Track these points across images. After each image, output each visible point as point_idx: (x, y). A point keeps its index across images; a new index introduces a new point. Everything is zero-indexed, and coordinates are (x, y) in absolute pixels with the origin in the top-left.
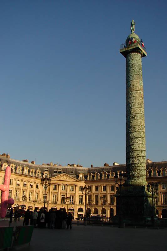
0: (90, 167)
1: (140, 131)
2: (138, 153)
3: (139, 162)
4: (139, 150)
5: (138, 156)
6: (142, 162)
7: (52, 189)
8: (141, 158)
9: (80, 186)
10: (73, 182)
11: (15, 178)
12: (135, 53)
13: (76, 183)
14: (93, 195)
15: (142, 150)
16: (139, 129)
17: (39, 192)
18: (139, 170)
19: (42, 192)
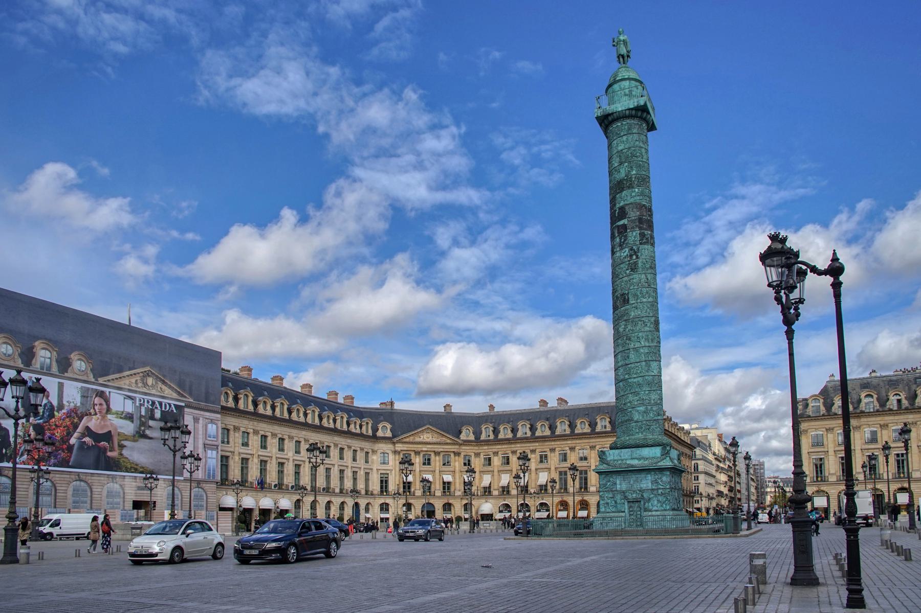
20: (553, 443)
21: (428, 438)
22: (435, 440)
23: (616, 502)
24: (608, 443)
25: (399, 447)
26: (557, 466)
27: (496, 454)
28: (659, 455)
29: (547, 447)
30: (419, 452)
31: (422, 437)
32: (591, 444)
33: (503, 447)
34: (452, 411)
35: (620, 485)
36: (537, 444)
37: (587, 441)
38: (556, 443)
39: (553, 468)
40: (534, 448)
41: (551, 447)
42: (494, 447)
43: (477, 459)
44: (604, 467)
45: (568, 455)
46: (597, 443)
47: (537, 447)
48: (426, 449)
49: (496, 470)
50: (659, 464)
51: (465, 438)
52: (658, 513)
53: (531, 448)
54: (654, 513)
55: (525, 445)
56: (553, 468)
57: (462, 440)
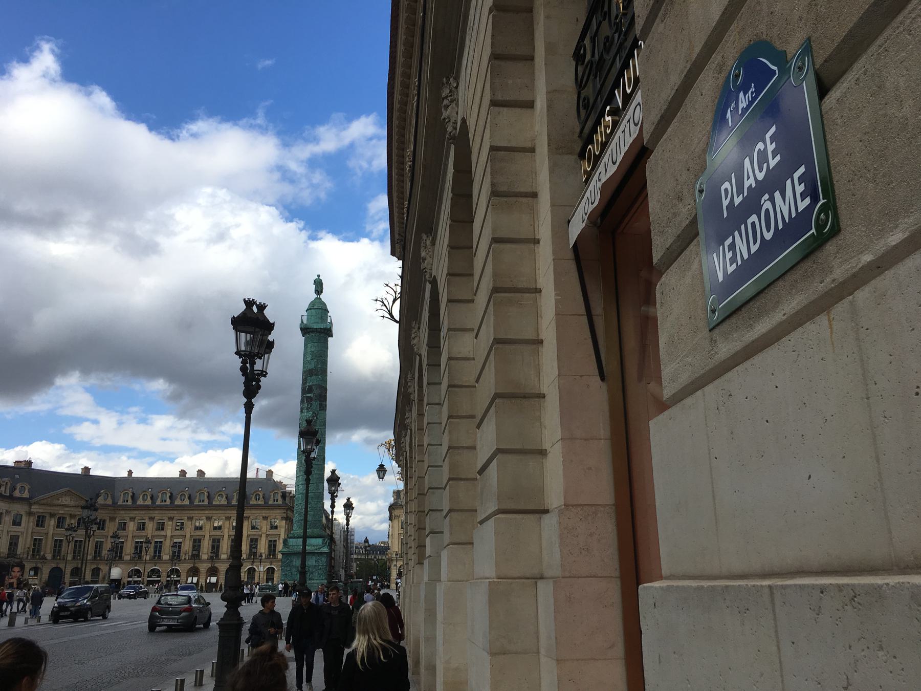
20: (191, 512)
21: (66, 501)
22: (73, 503)
23: (292, 574)
25: (35, 509)
26: (192, 534)
27: (133, 519)
28: (321, 543)
29: (186, 515)
30: (55, 515)
31: (61, 499)
32: (227, 515)
33: (141, 513)
34: (90, 474)
35: (296, 562)
36: (176, 512)
37: (223, 512)
38: (194, 512)
39: (188, 536)
40: (172, 516)
41: (188, 515)
42: (132, 512)
44: (286, 550)
48: (60, 512)
49: (130, 536)
50: (321, 550)
51: (102, 502)
52: (318, 581)
53: (169, 515)
54: (315, 581)
55: (163, 512)
56: (188, 536)
57: (101, 504)
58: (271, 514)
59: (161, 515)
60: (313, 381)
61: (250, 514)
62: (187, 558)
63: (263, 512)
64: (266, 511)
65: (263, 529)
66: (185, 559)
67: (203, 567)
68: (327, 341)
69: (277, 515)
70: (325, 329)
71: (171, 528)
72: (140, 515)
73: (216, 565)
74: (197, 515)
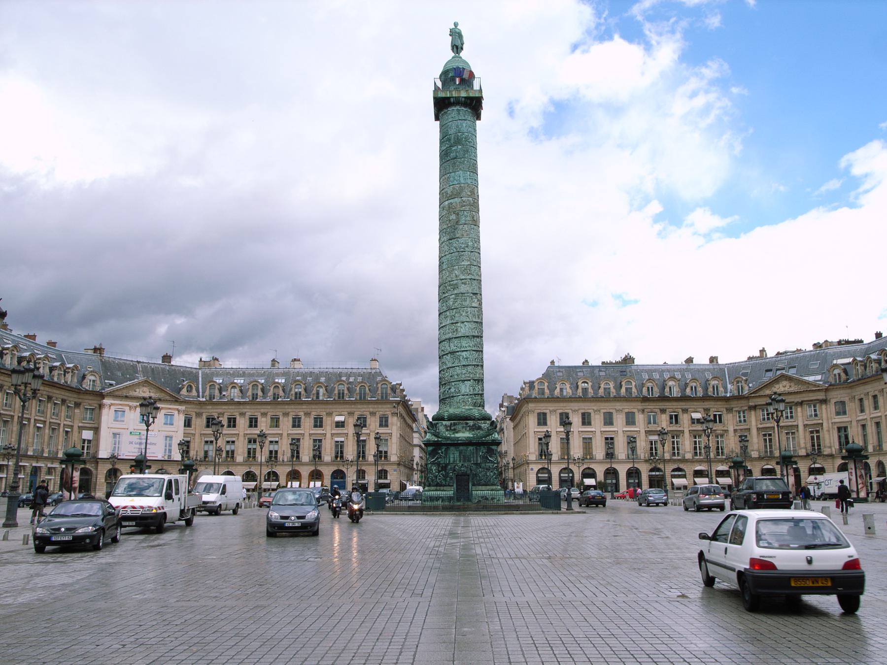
0: (874, 338)
1: (447, 295)
2: (443, 348)
3: (445, 367)
4: (444, 341)
5: (443, 353)
6: (450, 365)
7: (756, 420)
8: (448, 357)
9: (835, 400)
10: (811, 394)
11: (640, 407)
12: (443, 113)
13: (821, 396)
14: (869, 423)
15: (450, 339)
16: (444, 293)
17: (726, 431)
18: (445, 384)
19: (735, 431)
20: (286, 407)
24: (346, 410)
29: (280, 410)
36: (269, 407)
37: (324, 406)
38: (290, 407)
39: (285, 435)
43: (199, 420)
45: (302, 420)
46: (334, 410)
47: (269, 410)
55: (256, 407)
56: (285, 435)
58: (379, 410)
59: (253, 411)
60: (461, 176)
61: (355, 410)
62: (286, 460)
63: (370, 406)
64: (373, 406)
65: (371, 427)
66: (283, 461)
67: (305, 472)
68: (474, 123)
69: (387, 410)
70: (471, 99)
71: (265, 424)
72: (229, 411)
73: (319, 468)
74: (294, 410)
